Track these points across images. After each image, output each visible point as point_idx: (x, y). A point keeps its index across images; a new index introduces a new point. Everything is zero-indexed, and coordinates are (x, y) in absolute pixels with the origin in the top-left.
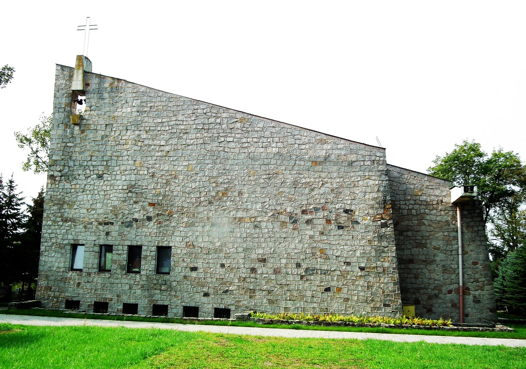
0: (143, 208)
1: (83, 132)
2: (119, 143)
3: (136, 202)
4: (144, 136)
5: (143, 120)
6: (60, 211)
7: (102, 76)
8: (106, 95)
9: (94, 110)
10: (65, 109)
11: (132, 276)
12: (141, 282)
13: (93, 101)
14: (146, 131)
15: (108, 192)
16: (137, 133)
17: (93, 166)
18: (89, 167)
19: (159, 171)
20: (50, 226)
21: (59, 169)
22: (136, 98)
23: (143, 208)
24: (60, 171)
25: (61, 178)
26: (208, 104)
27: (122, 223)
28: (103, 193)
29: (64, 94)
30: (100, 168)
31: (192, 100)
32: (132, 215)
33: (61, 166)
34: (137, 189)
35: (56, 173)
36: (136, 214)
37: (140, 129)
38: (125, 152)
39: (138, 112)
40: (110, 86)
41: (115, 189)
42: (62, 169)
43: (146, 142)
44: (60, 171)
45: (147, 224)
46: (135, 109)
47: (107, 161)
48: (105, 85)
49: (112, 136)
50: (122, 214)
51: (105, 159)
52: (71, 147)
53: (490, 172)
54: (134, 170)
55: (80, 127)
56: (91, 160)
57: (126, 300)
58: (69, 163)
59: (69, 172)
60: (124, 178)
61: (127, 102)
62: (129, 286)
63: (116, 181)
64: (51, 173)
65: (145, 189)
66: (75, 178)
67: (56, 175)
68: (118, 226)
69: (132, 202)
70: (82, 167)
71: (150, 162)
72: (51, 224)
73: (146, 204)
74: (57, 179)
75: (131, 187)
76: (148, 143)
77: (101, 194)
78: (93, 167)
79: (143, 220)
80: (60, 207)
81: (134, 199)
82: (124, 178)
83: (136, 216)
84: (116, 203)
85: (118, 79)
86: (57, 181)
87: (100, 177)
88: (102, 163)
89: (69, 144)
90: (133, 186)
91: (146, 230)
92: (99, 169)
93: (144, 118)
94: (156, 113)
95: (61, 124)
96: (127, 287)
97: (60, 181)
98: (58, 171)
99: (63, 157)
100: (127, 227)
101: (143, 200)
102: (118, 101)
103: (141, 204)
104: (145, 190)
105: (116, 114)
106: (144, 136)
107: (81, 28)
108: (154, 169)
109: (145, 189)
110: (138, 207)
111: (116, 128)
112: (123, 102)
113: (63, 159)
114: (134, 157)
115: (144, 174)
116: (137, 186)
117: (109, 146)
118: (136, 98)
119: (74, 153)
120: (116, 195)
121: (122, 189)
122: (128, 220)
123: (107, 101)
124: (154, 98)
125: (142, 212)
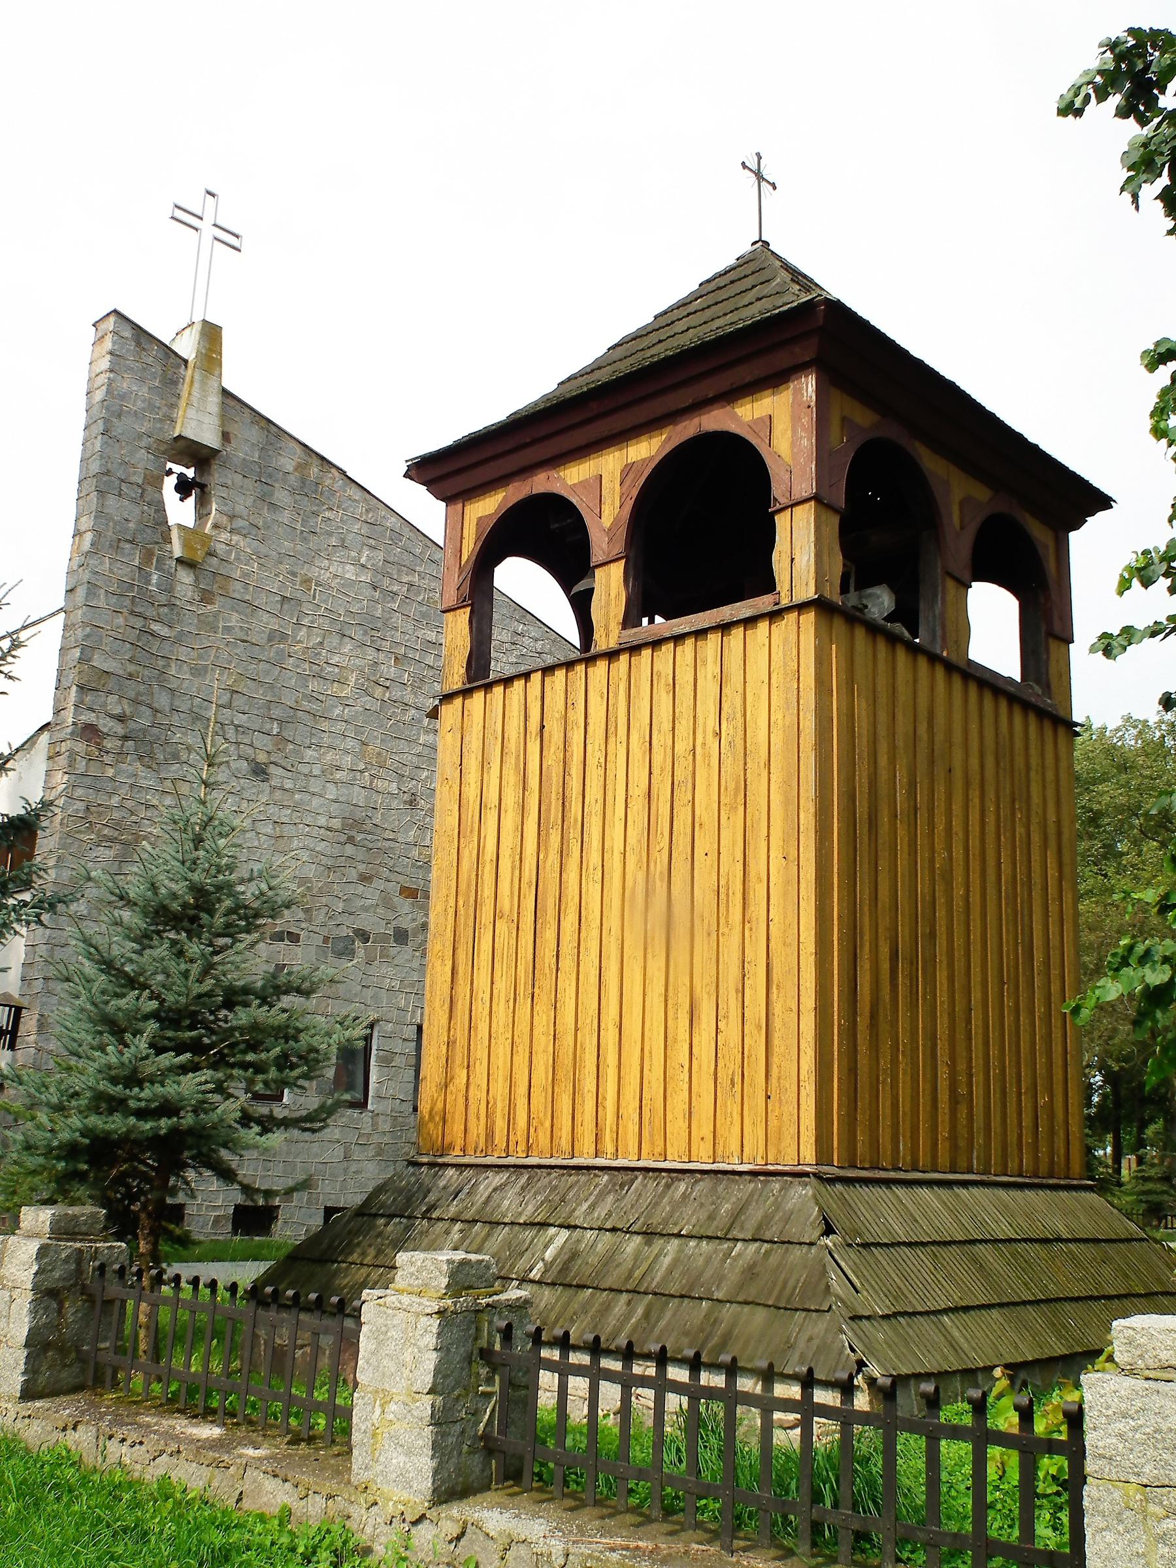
0: (387, 903)
1: (206, 597)
2: (321, 670)
3: (365, 879)
4: (389, 670)
5: (387, 620)
6: (120, 868)
7: (275, 429)
8: (282, 496)
9: (244, 532)
10: (144, 490)
11: (351, 1117)
12: (375, 1139)
13: (240, 499)
14: (396, 658)
15: (286, 828)
16: (371, 654)
17: (237, 726)
18: (222, 729)
19: (428, 791)
20: (82, 918)
21: (117, 710)
22: (373, 542)
23: (387, 903)
24: (121, 718)
25: (122, 746)
26: (546, 629)
27: (326, 939)
28: (268, 829)
29: (140, 436)
30: (260, 741)
31: (512, 603)
32: (352, 917)
33: (125, 701)
34: (369, 837)
35: (106, 725)
36: (364, 915)
37: (379, 643)
38: (336, 707)
39: (375, 588)
40: (296, 470)
41: (304, 822)
42: (128, 713)
43: (396, 693)
44: (121, 718)
45: (393, 951)
46: (366, 577)
47: (281, 722)
48: (282, 460)
49: (300, 642)
50: (324, 910)
51: (276, 712)
52: (164, 639)
53: (628, 1365)
54: (361, 772)
55: (197, 579)
56: (229, 706)
57: (333, 1197)
58: (156, 696)
59: (155, 731)
60: (332, 792)
61: (343, 546)
62: (342, 1150)
63: (307, 797)
64: (88, 717)
65: (389, 840)
66: (176, 756)
67: (105, 730)
68: (313, 949)
69: (353, 875)
70: (199, 723)
71: (406, 758)
72: (85, 912)
73: (393, 888)
74: (108, 744)
75: (352, 827)
76: (402, 696)
77: (263, 831)
78: (237, 730)
79: (383, 938)
80: (123, 856)
81: (362, 868)
82: (332, 792)
83: (365, 921)
84: (311, 871)
85: (323, 458)
86: (108, 753)
87: (260, 771)
88: (267, 726)
89: (155, 627)
90: (357, 824)
91: (391, 971)
92: (257, 744)
93: (390, 613)
94: (424, 609)
95: (127, 541)
96: (339, 1152)
97: (121, 754)
98: (112, 716)
99: (131, 668)
100: (339, 954)
101: (385, 873)
102: (318, 530)
103: (378, 884)
104: (391, 844)
105: (314, 572)
106: (389, 670)
107: (185, 217)
108: (414, 782)
109: (389, 840)
110: (371, 894)
111: (310, 618)
112: (334, 541)
113: (130, 675)
114: (363, 729)
115: (388, 793)
116: (369, 827)
117: (291, 674)
118: (373, 542)
119: (173, 665)
120: (309, 842)
121: (328, 829)
122: (345, 932)
123: (285, 517)
124: (419, 561)
125: (380, 910)
